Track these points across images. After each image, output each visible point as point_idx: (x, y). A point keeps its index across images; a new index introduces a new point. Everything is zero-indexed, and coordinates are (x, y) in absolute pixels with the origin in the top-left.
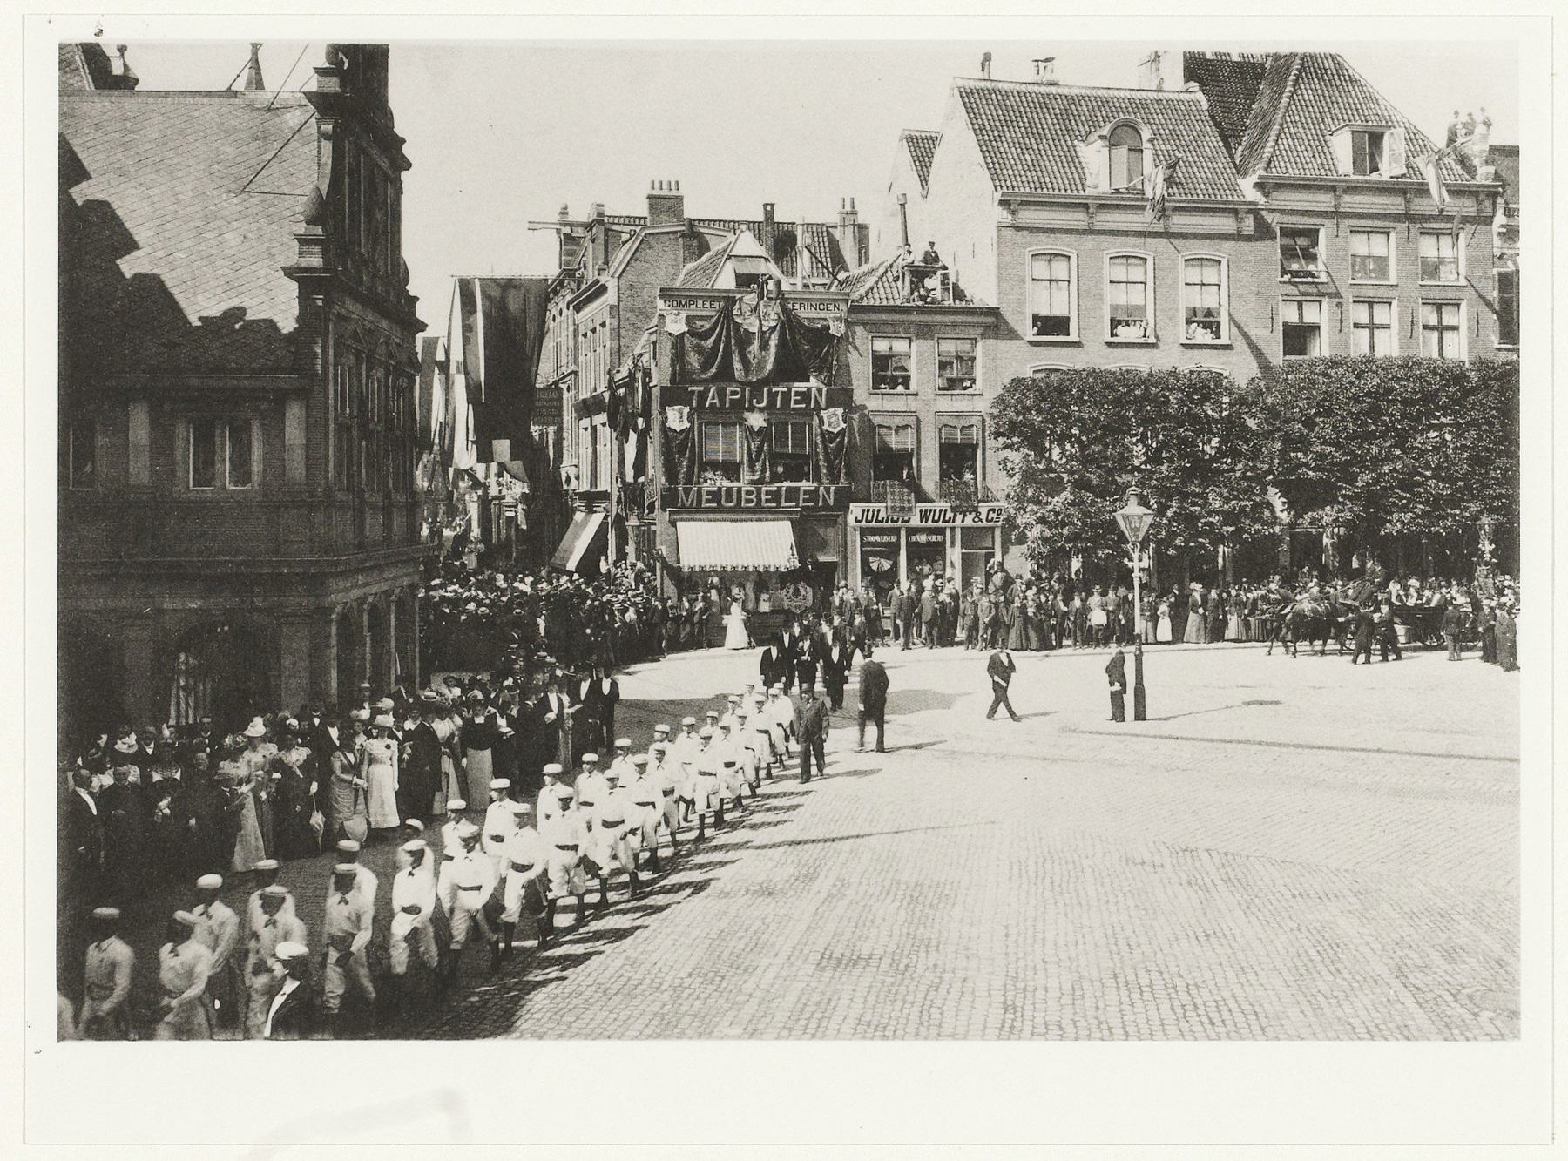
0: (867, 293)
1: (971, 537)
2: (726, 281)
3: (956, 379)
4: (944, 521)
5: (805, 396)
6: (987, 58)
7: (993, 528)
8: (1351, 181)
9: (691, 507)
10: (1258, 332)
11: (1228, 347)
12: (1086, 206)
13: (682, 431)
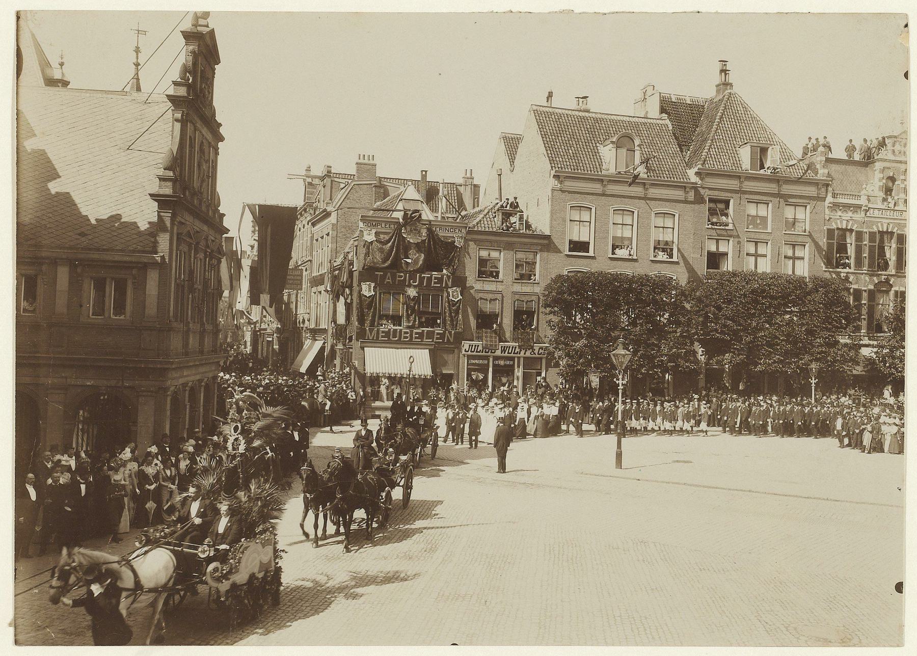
0: (477, 224)
1: (530, 363)
3: (525, 274)
5: (440, 280)
6: (550, 95)
8: (750, 173)
11: (677, 263)
12: (602, 181)
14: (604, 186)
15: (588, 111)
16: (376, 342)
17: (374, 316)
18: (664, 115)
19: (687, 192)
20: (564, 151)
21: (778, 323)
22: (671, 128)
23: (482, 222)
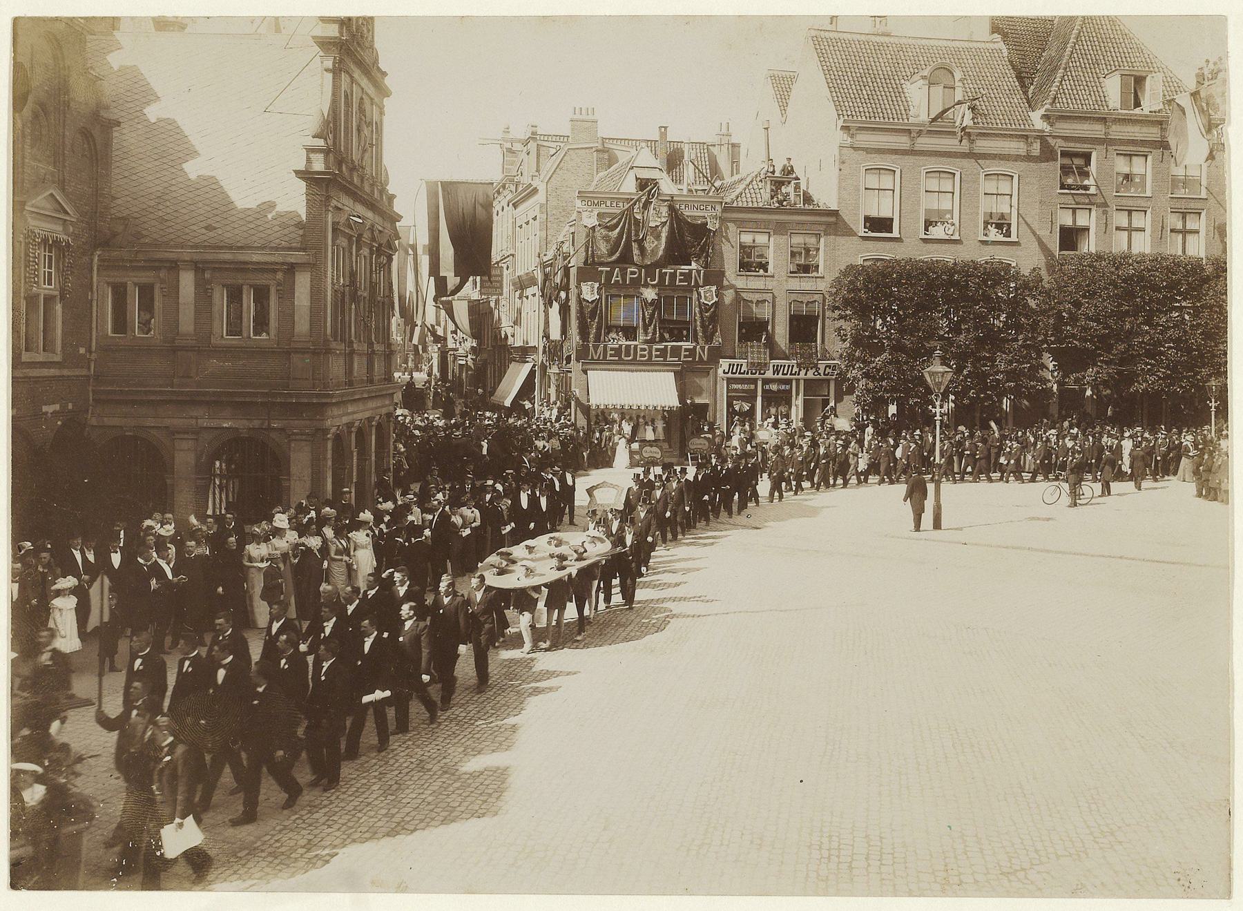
1: (811, 386)
5: (687, 276)
7: (828, 381)
8: (1119, 114)
10: (1044, 233)
13: (593, 301)
15: (888, 35)
16: (603, 362)
17: (599, 329)
18: (996, 35)
22: (1006, 54)
23: (744, 194)
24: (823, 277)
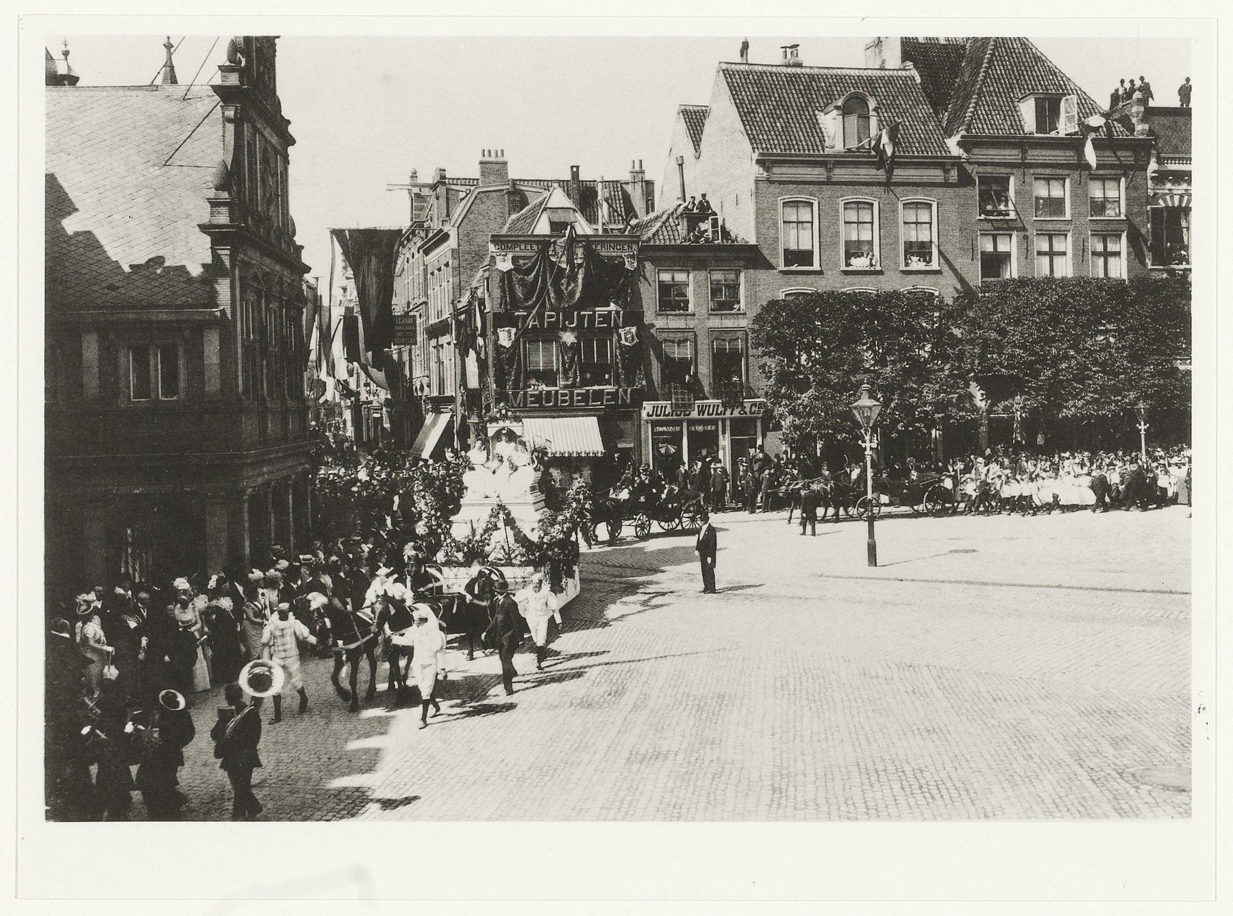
0: (654, 235)
2: (543, 227)
3: (724, 300)
4: (717, 414)
5: (607, 317)
6: (745, 46)
7: (754, 420)
9: (519, 406)
11: (939, 272)
14: (829, 170)
19: (946, 171)
20: (769, 125)
21: (1087, 348)
24: (745, 314)
